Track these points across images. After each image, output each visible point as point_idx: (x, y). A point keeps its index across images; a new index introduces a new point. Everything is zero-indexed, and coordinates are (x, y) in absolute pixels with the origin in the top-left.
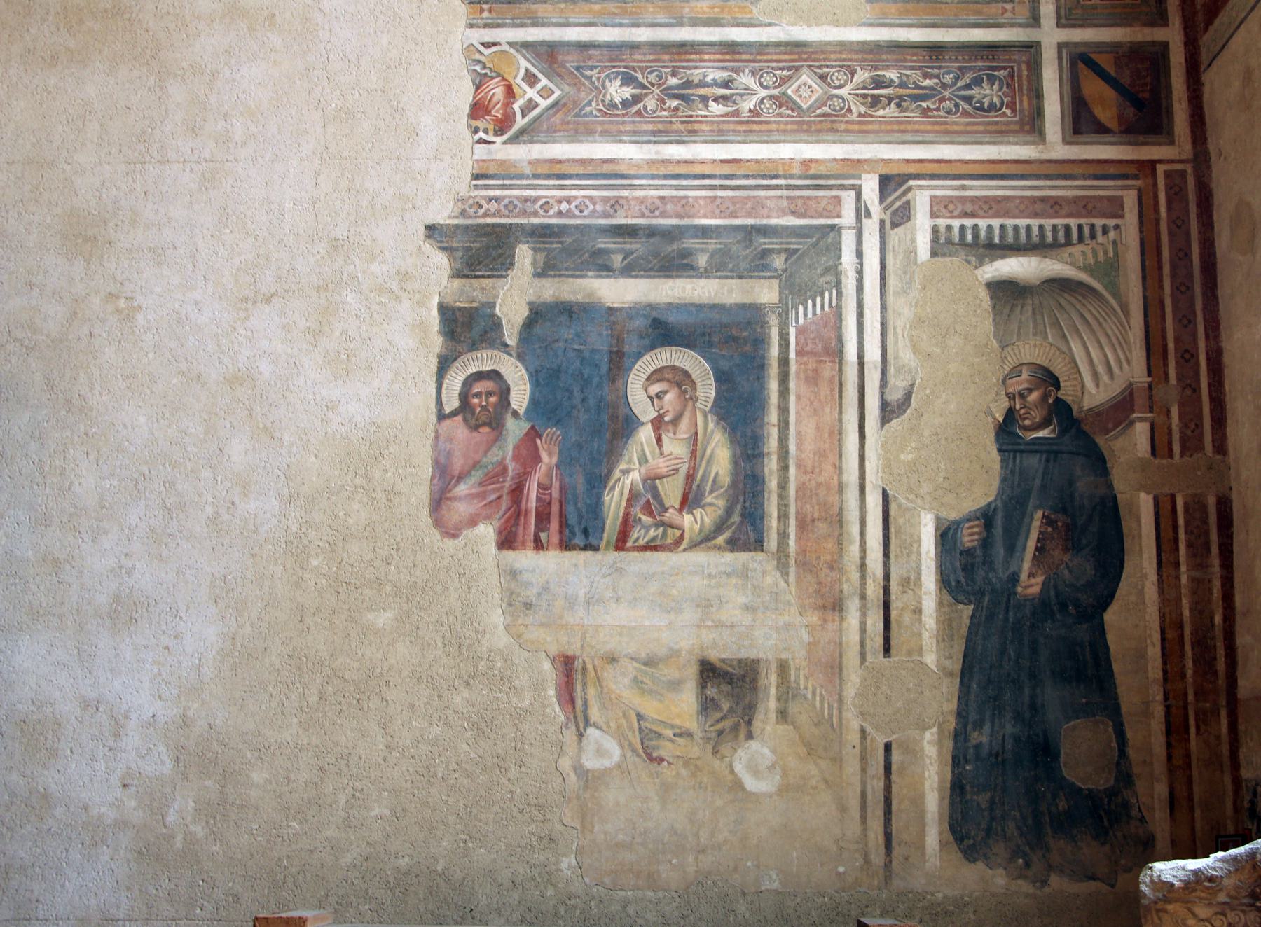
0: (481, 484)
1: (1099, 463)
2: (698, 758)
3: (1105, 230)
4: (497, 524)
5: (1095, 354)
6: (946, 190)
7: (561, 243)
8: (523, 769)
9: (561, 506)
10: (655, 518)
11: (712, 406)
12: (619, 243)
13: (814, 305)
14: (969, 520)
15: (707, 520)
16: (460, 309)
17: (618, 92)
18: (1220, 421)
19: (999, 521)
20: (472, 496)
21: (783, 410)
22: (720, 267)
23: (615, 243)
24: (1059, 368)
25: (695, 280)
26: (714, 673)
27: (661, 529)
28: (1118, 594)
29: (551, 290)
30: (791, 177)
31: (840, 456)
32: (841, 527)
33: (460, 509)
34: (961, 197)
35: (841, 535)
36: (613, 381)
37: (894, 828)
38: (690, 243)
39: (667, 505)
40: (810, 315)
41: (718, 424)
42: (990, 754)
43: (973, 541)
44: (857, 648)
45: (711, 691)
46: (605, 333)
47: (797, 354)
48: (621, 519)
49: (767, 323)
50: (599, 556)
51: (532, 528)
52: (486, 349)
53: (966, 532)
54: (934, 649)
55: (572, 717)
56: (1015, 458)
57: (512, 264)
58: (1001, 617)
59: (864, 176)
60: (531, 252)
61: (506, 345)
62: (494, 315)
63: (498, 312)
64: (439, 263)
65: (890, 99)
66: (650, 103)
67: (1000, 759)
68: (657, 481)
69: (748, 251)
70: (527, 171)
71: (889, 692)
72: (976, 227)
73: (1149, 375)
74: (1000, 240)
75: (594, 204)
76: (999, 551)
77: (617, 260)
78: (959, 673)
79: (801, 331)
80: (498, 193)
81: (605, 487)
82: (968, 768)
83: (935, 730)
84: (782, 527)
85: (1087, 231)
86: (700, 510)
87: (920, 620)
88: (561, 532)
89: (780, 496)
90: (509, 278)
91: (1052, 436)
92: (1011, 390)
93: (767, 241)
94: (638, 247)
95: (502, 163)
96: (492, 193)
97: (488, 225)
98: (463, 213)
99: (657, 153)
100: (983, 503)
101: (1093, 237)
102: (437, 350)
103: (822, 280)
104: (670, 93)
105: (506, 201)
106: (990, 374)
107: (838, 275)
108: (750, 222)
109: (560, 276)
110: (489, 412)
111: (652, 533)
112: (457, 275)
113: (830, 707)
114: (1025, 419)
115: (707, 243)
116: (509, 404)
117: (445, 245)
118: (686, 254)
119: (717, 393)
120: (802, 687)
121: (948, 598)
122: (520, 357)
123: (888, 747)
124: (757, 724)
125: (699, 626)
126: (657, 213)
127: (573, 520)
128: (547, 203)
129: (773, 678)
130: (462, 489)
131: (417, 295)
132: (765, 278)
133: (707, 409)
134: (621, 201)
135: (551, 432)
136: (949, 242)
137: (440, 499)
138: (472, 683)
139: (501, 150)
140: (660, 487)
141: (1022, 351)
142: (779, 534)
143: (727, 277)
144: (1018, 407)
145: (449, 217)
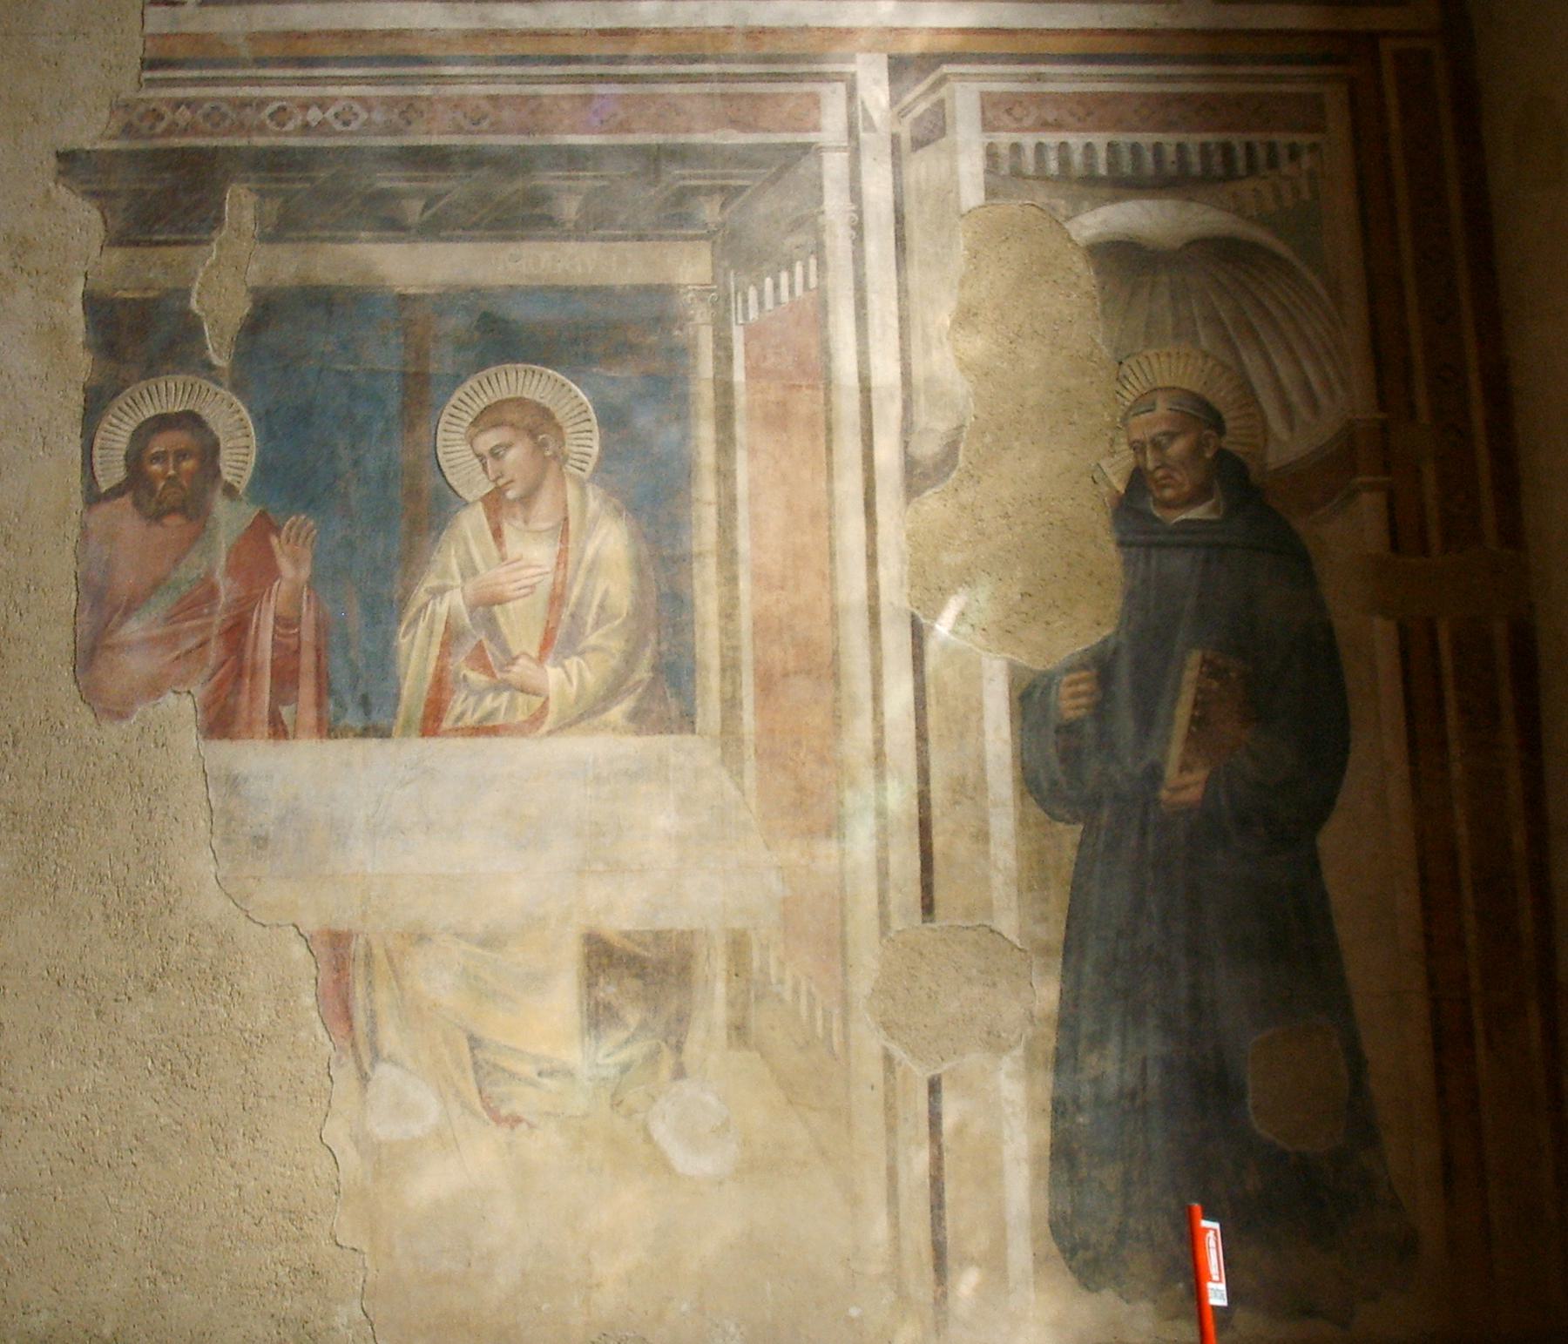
0: (170, 619)
2: (586, 1116)
3: (1294, 154)
4: (199, 690)
5: (1285, 372)
6: (1004, 80)
7: (308, 179)
8: (259, 1144)
9: (319, 657)
10: (493, 675)
11: (595, 470)
12: (415, 179)
13: (776, 287)
14: (1069, 670)
15: (590, 677)
16: (125, 302)
18: (1509, 487)
19: (1123, 670)
20: (153, 642)
23: (409, 180)
24: (1221, 396)
25: (556, 244)
26: (610, 956)
27: (506, 696)
28: (1339, 801)
30: (730, 59)
31: (832, 556)
32: (838, 684)
33: (137, 665)
34: (1037, 94)
35: (836, 700)
36: (411, 427)
37: (949, 1233)
39: (516, 652)
40: (769, 305)
41: (605, 501)
42: (1121, 1094)
43: (1078, 707)
44: (873, 906)
45: (608, 991)
46: (393, 342)
47: (748, 376)
48: (430, 679)
49: (691, 319)
50: (390, 746)
51: (266, 697)
52: (174, 373)
53: (1065, 691)
54: (1014, 904)
55: (347, 1044)
56: (1148, 557)
57: (219, 220)
58: (1133, 843)
59: (860, 57)
60: (255, 198)
61: (209, 366)
62: (186, 313)
63: (194, 305)
67: (1138, 1102)
68: (496, 609)
69: (652, 192)
70: (245, 52)
71: (934, 987)
72: (1063, 146)
73: (1382, 405)
74: (1109, 171)
75: (369, 110)
76: (1125, 725)
77: (414, 210)
78: (1060, 947)
79: (752, 333)
80: (192, 92)
81: (400, 622)
82: (1081, 1120)
83: (1019, 1052)
84: (729, 688)
85: (1261, 154)
86: (575, 659)
87: (986, 854)
88: (319, 705)
89: (724, 631)
90: (214, 245)
91: (1213, 517)
92: (1136, 436)
93: (686, 172)
94: (455, 187)
95: (198, 39)
96: (179, 93)
97: (174, 150)
98: (128, 130)
99: (482, 18)
100: (1093, 638)
101: (1273, 163)
102: (83, 377)
103: (791, 241)
105: (207, 106)
106: (1099, 407)
107: (818, 231)
108: (655, 138)
109: (309, 239)
110: (182, 488)
111: (489, 703)
112: (117, 240)
113: (827, 1018)
114: (1164, 486)
115: (578, 178)
116: (218, 473)
117: (95, 187)
118: (537, 198)
119: (603, 447)
120: (774, 980)
121: (1036, 812)
122: (237, 387)
123: (934, 1087)
124: (692, 1048)
125: (580, 872)
126: (485, 125)
127: (341, 679)
128: (283, 109)
129: (720, 964)
130: (134, 629)
131: (44, 280)
132: (686, 238)
133: (585, 476)
134: (423, 106)
135: (298, 522)
136: (1017, 173)
137: (93, 649)
138: (160, 986)
140: (501, 620)
141: (1156, 366)
142: (723, 701)
143: (615, 239)
144: (1150, 465)
145: (102, 136)
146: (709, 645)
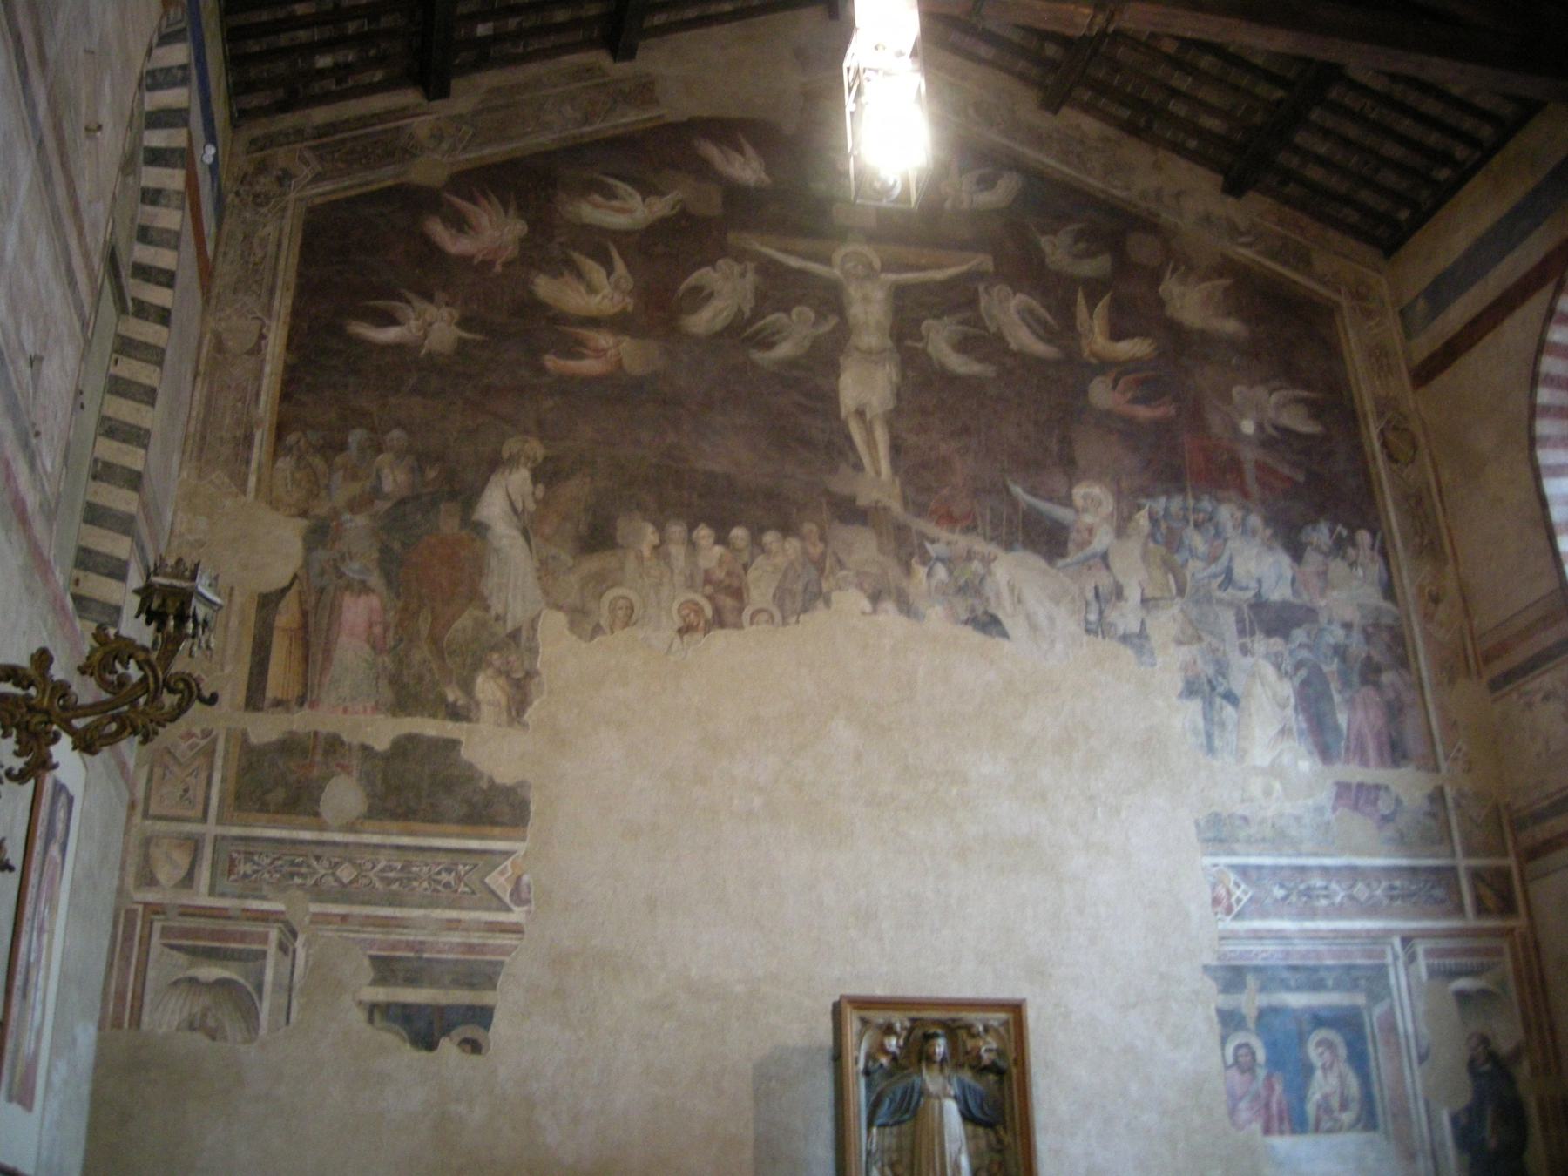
1: (1510, 1080)
17: (1279, 893)
21: (1377, 1059)
22: (1338, 986)
29: (1263, 1000)
38: (1322, 974)
57: (1245, 987)
64: (1210, 986)
65: (1398, 896)
66: (1294, 898)
77: (1292, 983)
95: (1232, 931)
98: (1219, 959)
104: (1301, 894)
139: (1229, 924)
146: (1379, 1110)
